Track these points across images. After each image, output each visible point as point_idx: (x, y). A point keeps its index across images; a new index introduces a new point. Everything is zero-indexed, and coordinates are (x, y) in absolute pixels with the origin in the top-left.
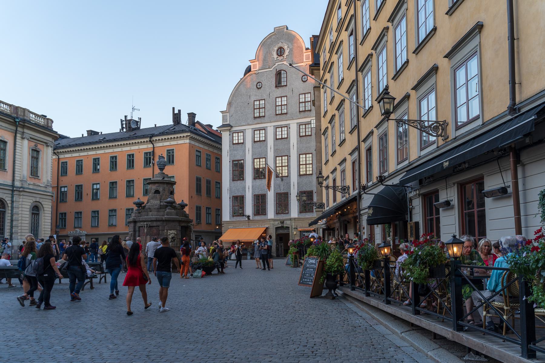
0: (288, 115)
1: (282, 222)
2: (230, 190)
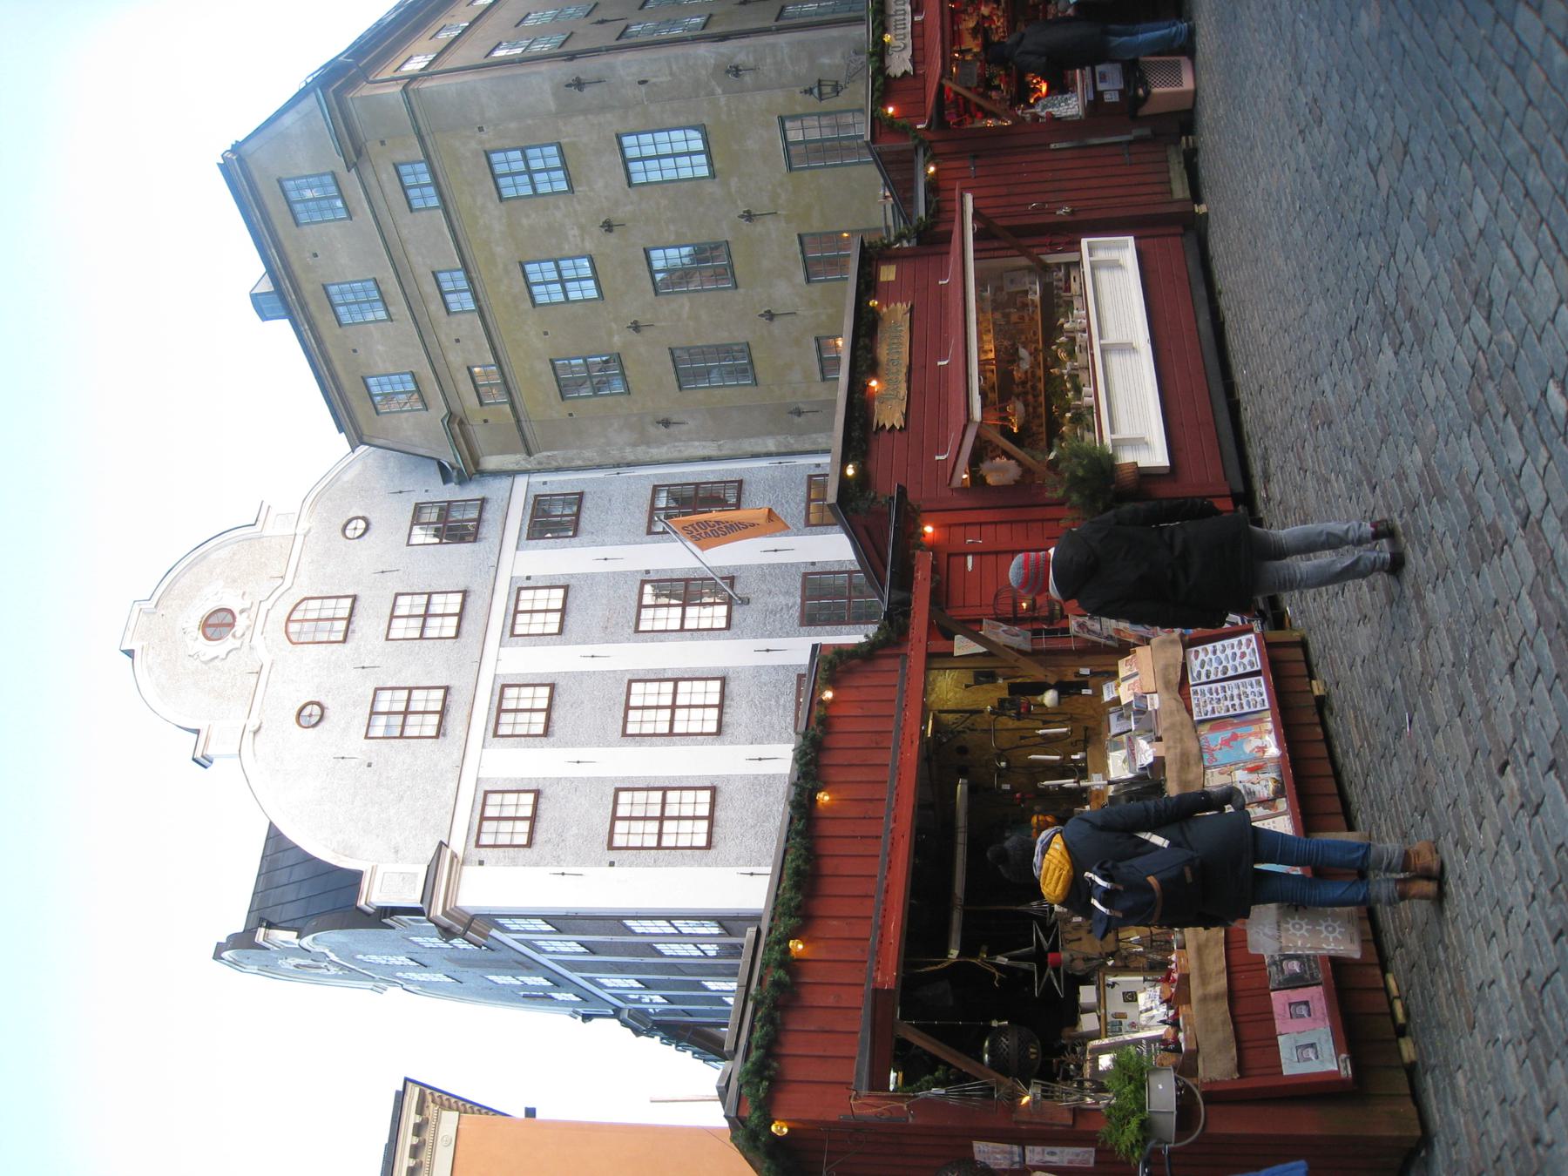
0: (474, 587)
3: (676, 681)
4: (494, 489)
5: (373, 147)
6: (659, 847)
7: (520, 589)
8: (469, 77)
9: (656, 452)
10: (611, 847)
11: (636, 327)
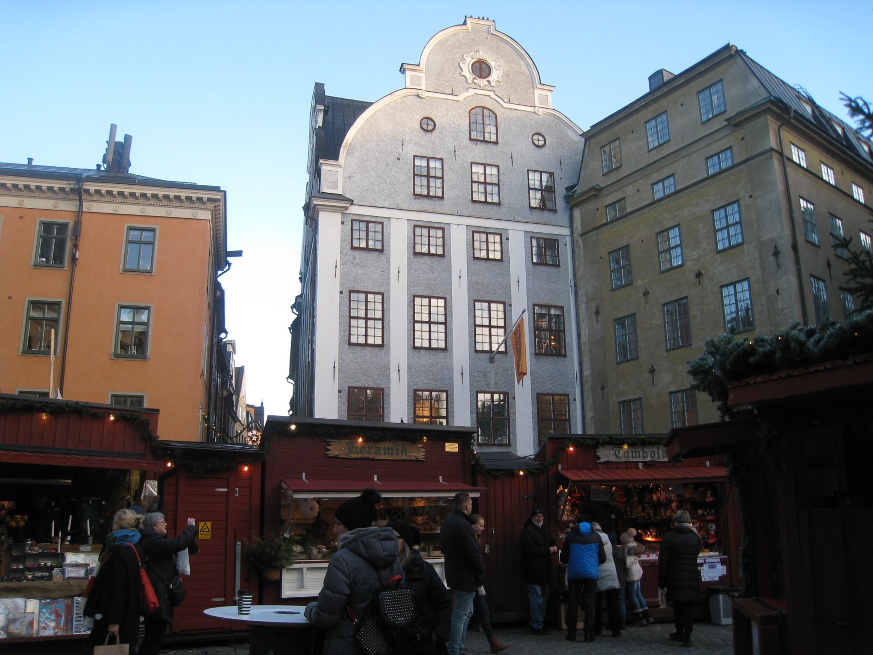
0: (503, 209)
2: (342, 368)
3: (445, 323)
4: (562, 216)
5: (740, 133)
6: (350, 318)
7: (501, 235)
8: (781, 187)
9: (582, 307)
10: (351, 292)
11: (646, 293)
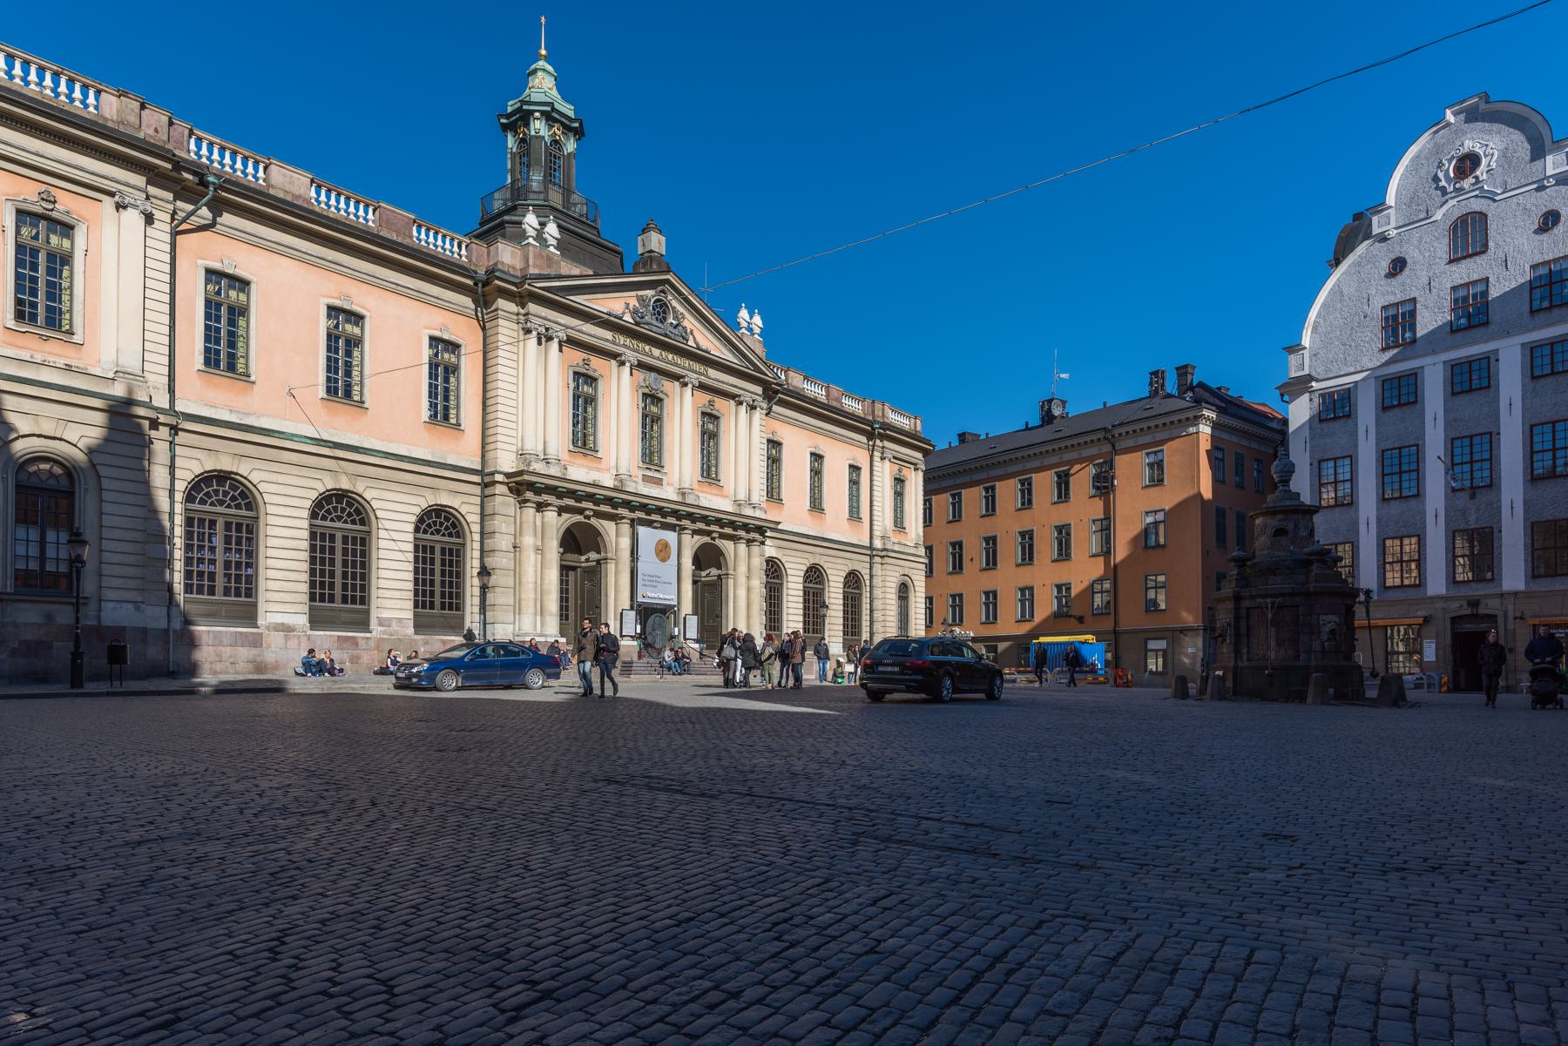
0: (1491, 327)
1: (1474, 603)
